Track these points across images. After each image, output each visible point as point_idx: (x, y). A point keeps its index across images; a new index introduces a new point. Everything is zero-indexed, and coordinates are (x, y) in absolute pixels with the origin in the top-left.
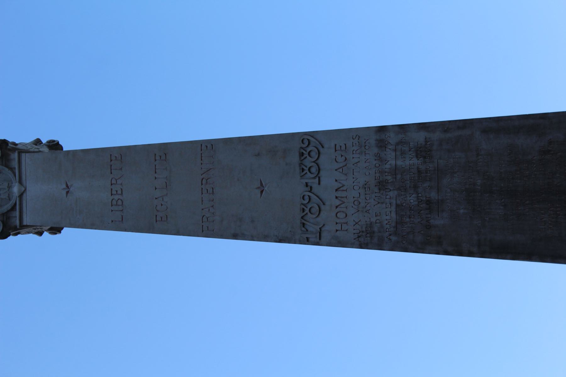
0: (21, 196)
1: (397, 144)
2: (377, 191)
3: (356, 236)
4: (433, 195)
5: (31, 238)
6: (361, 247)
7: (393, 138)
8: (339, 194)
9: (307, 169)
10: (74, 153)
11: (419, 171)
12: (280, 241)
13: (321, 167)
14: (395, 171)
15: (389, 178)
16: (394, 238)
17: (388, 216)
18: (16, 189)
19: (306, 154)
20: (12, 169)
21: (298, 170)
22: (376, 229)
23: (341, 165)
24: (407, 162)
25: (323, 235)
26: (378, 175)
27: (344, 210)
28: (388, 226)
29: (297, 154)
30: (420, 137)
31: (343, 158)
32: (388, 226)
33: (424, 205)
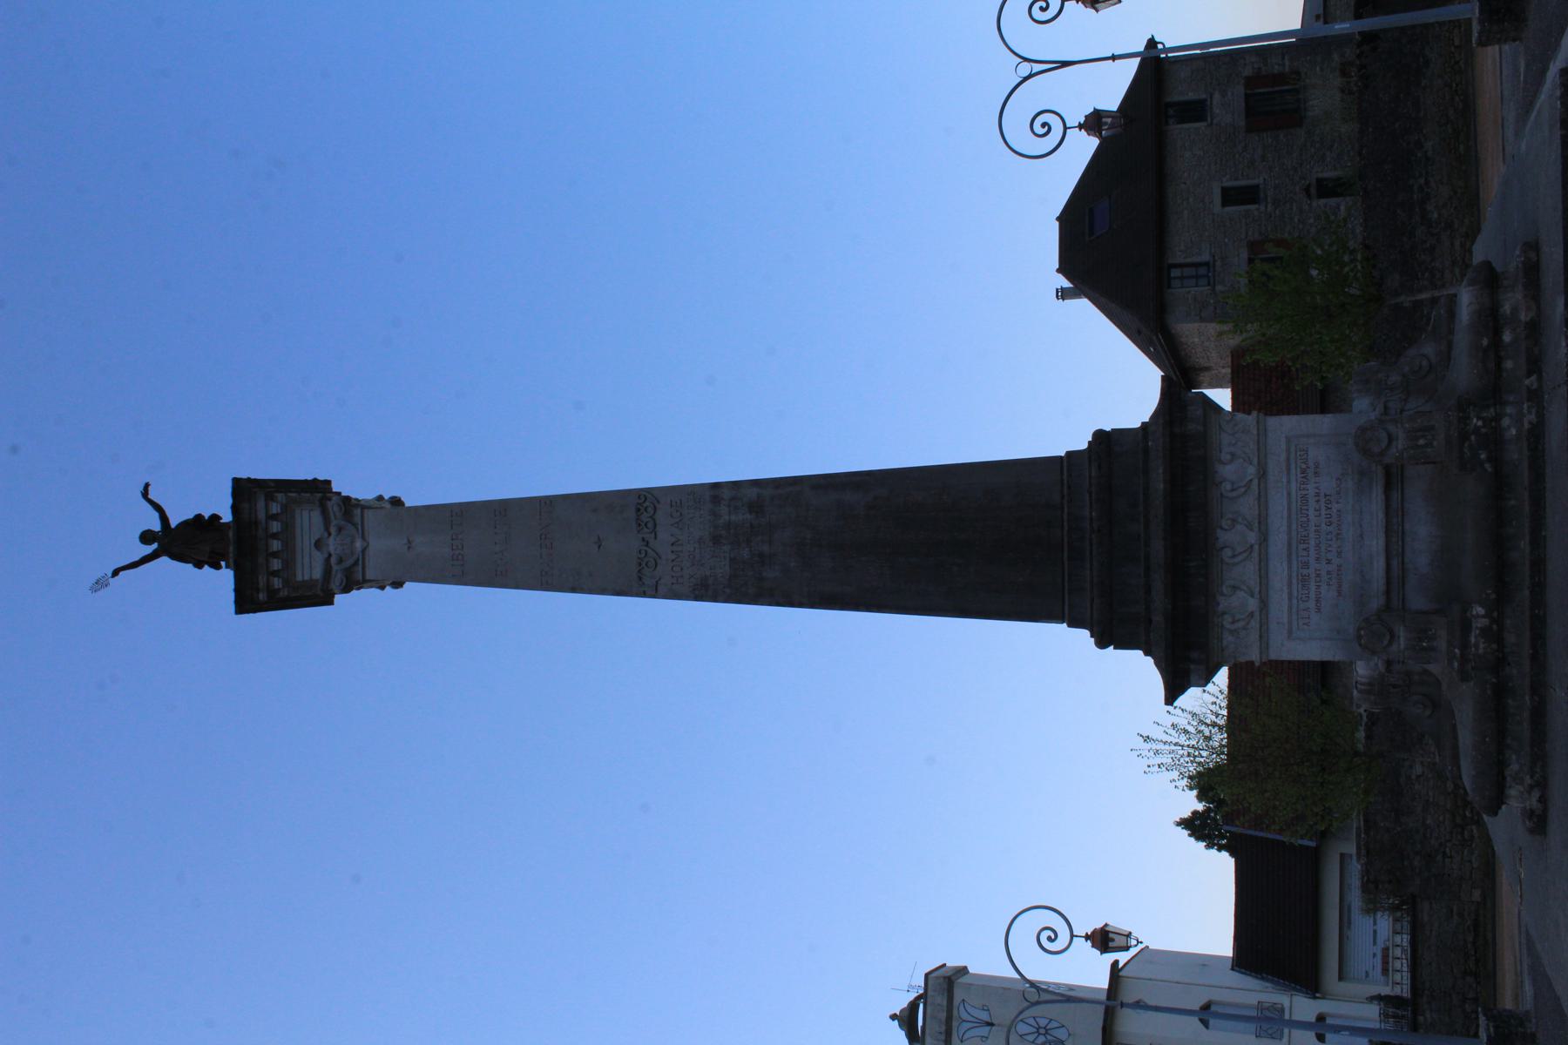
0: (364, 551)
5: (374, 591)
10: (416, 508)
18: (358, 544)
20: (355, 525)
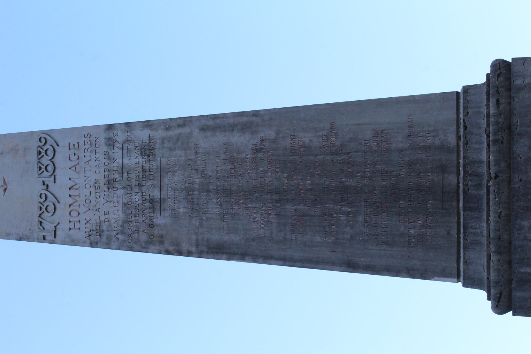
1: (124, 142)
2: (106, 189)
3: (87, 234)
4: (156, 194)
6: (91, 245)
7: (120, 136)
8: (72, 192)
9: (43, 167)
11: (144, 170)
12: (20, 239)
13: (57, 166)
14: (122, 169)
15: (116, 176)
16: (120, 237)
17: (116, 215)
19: (43, 153)
21: (36, 169)
22: (104, 228)
23: (74, 163)
24: (133, 161)
25: (57, 233)
26: (106, 173)
27: (77, 208)
28: (115, 225)
29: (36, 153)
30: (143, 135)
31: (76, 156)
32: (115, 225)
33: (148, 204)
